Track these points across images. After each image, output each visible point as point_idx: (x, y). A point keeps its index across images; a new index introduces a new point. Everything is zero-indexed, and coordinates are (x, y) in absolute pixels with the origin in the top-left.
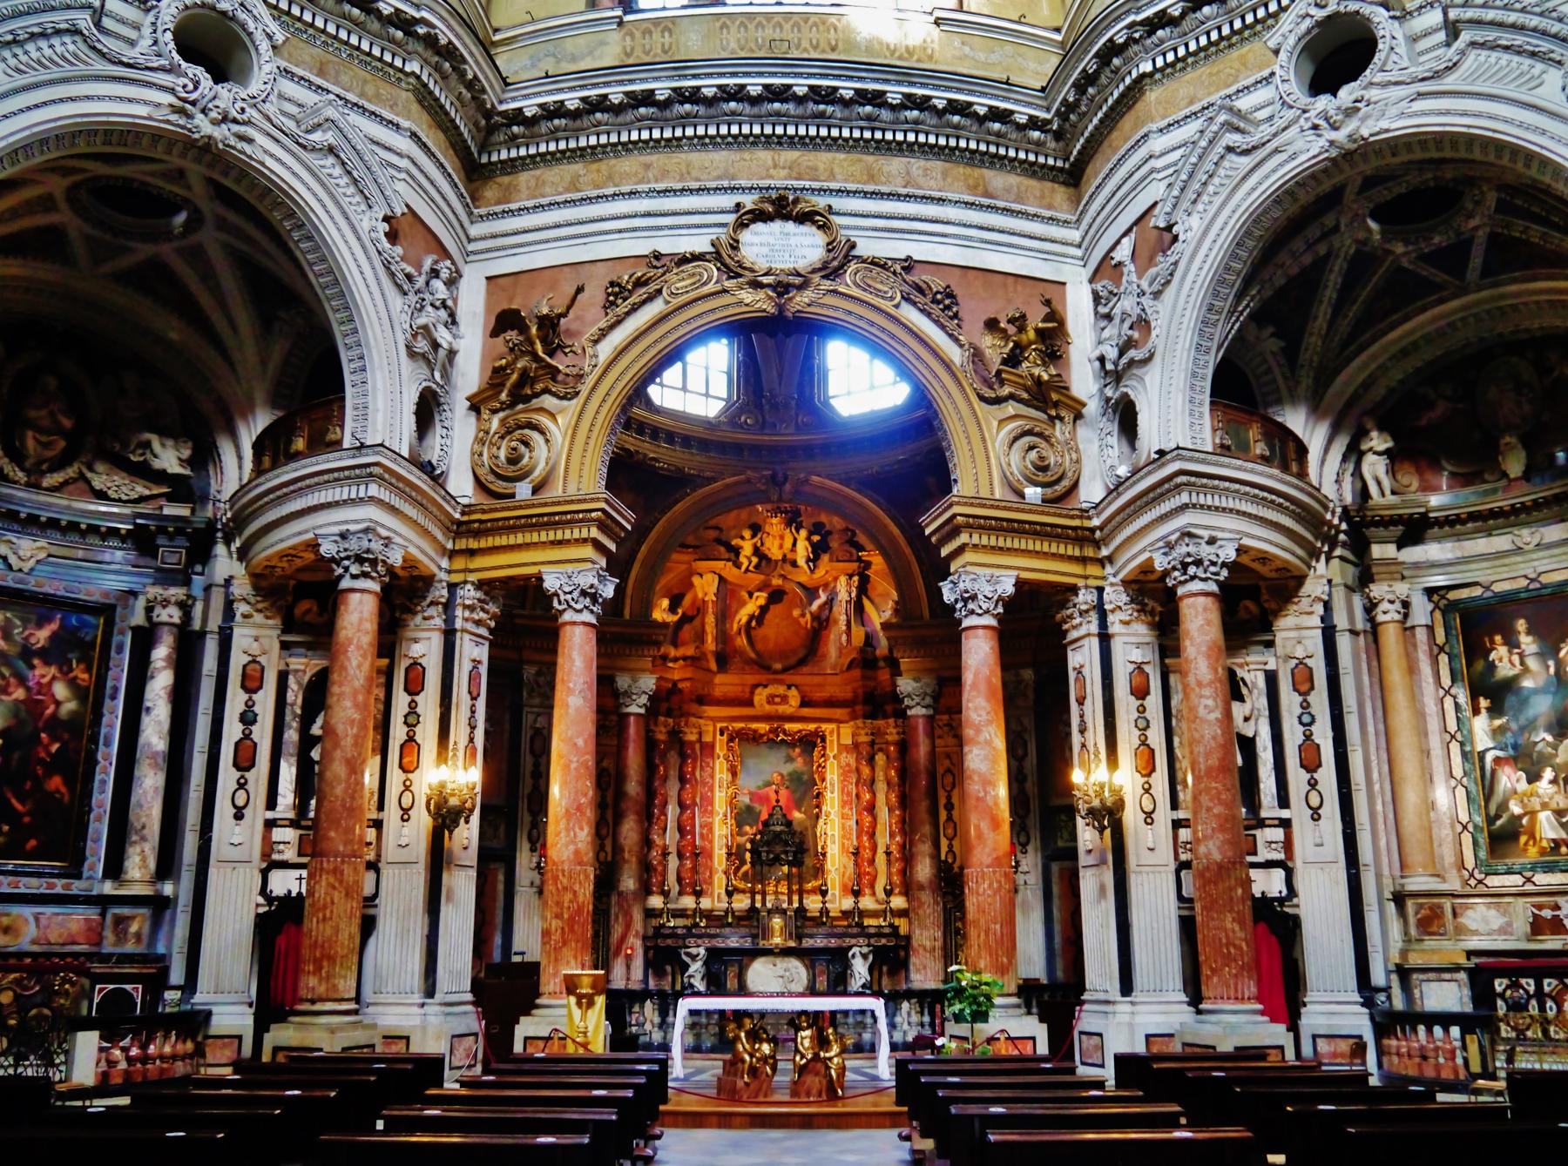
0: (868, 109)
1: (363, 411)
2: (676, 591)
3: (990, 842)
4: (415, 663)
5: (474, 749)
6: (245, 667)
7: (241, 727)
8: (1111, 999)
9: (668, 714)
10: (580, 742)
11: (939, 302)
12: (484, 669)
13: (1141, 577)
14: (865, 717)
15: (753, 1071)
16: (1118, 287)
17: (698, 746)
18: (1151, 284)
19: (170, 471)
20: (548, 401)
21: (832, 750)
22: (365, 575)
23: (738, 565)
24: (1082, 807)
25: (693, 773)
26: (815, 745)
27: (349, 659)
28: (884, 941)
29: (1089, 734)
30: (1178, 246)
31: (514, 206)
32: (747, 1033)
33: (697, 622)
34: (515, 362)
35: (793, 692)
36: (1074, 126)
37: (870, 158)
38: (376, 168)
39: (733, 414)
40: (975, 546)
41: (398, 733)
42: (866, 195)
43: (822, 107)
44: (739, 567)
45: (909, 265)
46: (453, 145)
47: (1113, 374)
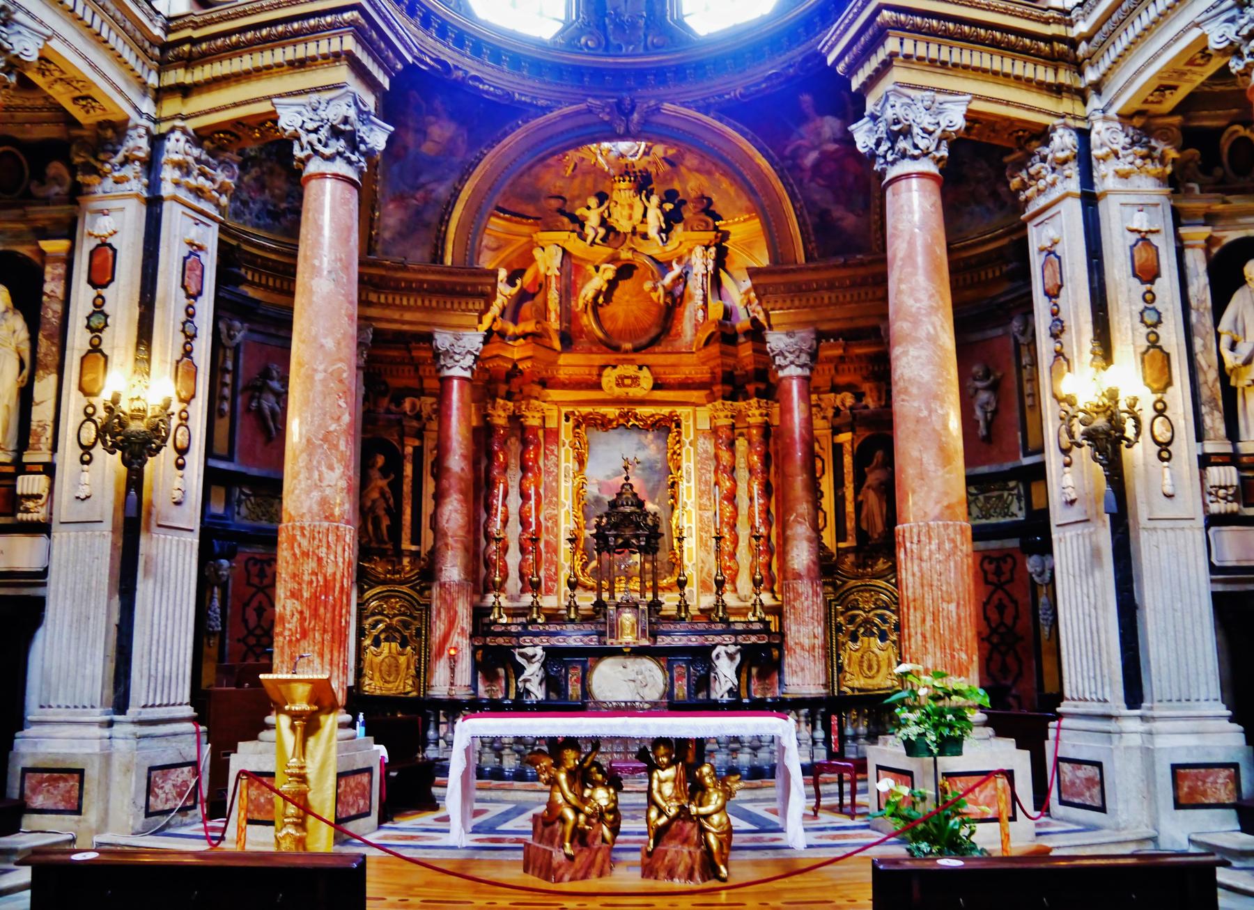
2: (516, 267)
3: (937, 483)
4: (104, 244)
8: (1114, 712)
9: (509, 396)
10: (329, 343)
12: (210, 260)
14: (725, 398)
15: (580, 837)
17: (541, 433)
21: (688, 434)
23: (583, 237)
25: (536, 460)
26: (669, 431)
28: (753, 639)
29: (1068, 338)
32: (571, 774)
33: (539, 299)
39: (570, 38)
40: (908, 57)
41: (78, 339)
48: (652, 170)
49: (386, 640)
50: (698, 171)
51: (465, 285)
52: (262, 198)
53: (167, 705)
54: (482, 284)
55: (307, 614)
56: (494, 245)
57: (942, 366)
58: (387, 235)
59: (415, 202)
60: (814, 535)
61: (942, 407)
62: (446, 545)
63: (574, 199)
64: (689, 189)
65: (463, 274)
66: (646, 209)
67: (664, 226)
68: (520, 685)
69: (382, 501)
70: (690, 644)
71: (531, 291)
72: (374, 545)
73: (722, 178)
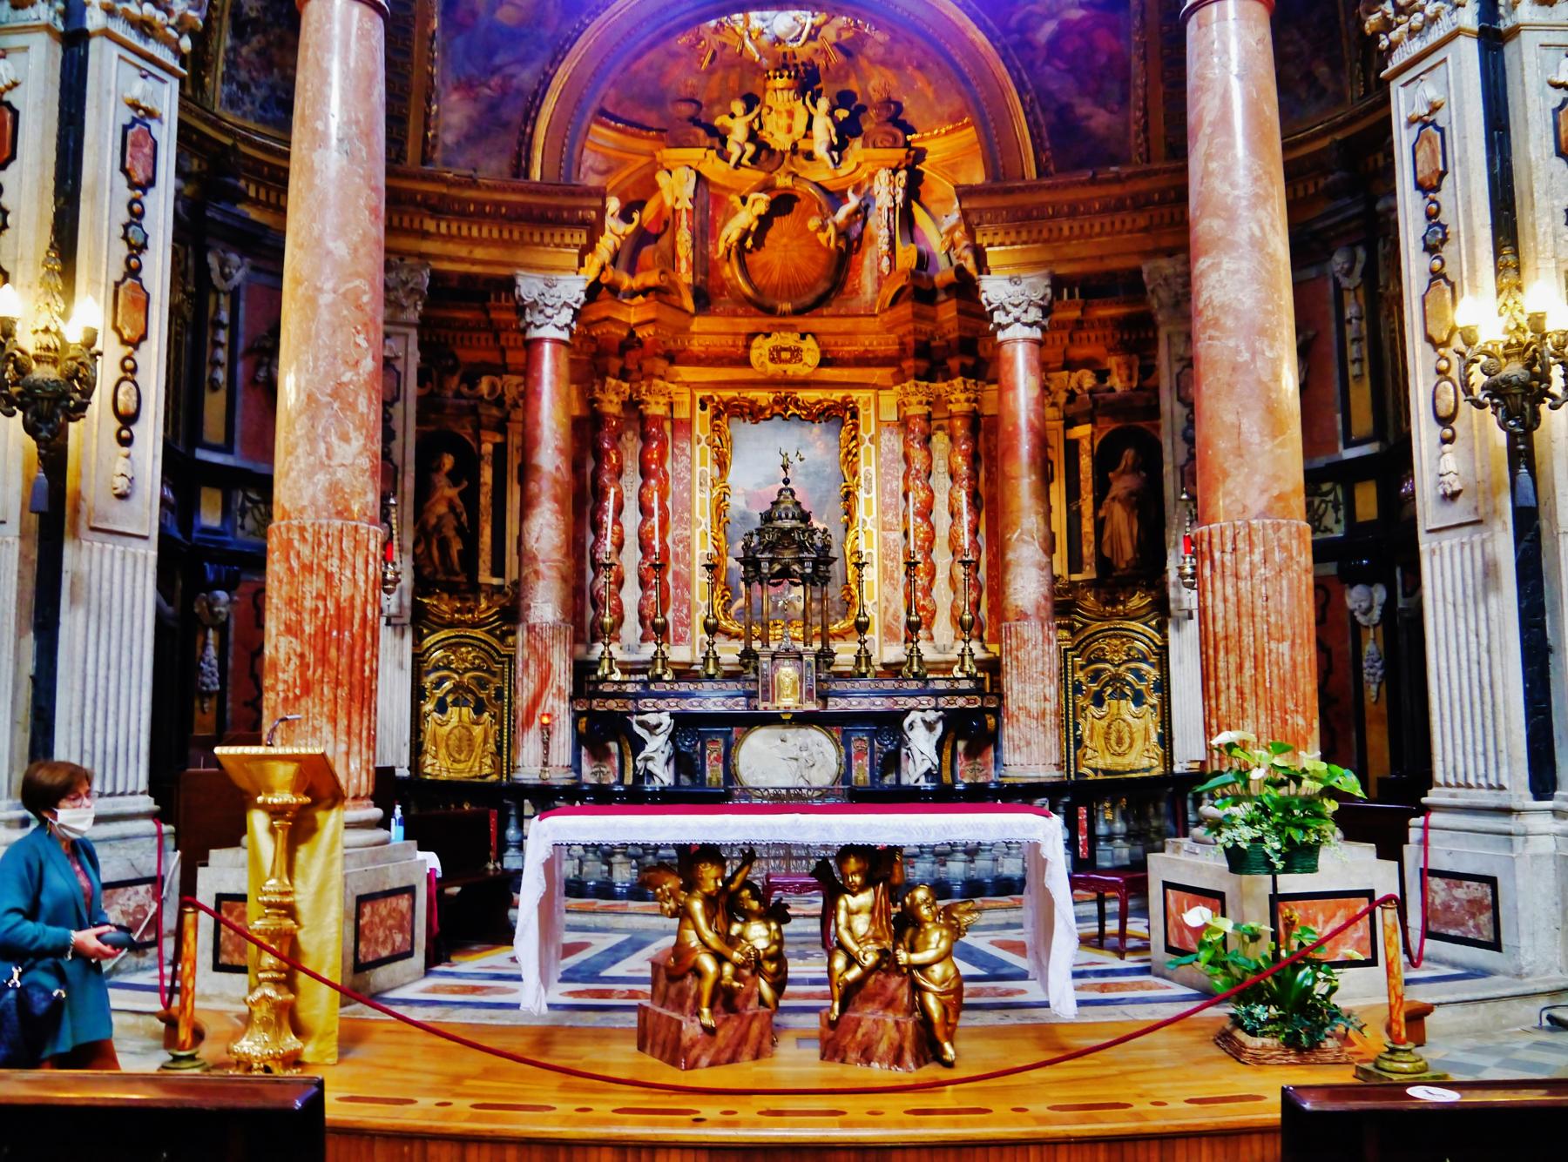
2: (632, 197)
8: (1515, 804)
9: (624, 375)
10: (340, 248)
14: (918, 377)
15: (725, 998)
17: (667, 426)
28: (961, 702)
32: (709, 900)
33: (664, 242)
35: (810, 342)
44: (727, 160)
48: (820, 62)
49: (455, 703)
50: (883, 63)
51: (559, 208)
52: (270, 81)
53: (110, 795)
54: (584, 208)
55: (310, 658)
56: (603, 167)
57: (1272, 285)
58: (449, 138)
59: (487, 91)
60: (1045, 559)
61: (1271, 347)
62: (536, 572)
63: (711, 103)
64: (870, 89)
65: (556, 194)
66: (811, 117)
67: (836, 141)
68: (640, 765)
69: (451, 517)
70: (873, 708)
71: (653, 230)
72: (441, 577)
73: (917, 74)
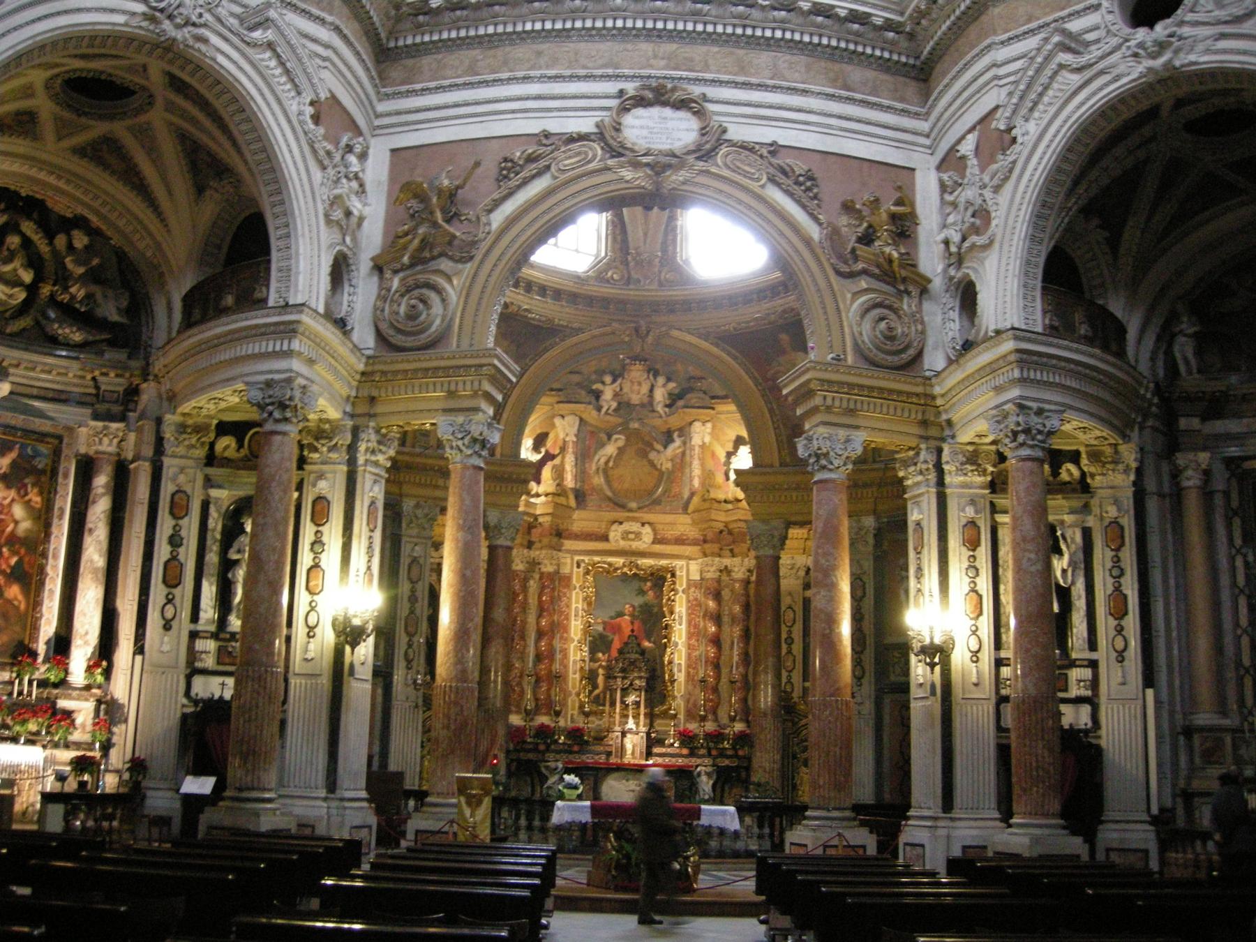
0: (741, 8)
1: (287, 273)
5: (371, 575)
6: (173, 495)
7: (169, 548)
11: (801, 184)
12: (380, 505)
13: (977, 440)
16: (963, 178)
18: (992, 179)
19: (110, 319)
20: (445, 264)
21: (681, 585)
22: (286, 420)
23: (599, 409)
24: (916, 646)
26: (664, 579)
27: (272, 494)
29: (925, 580)
30: (1017, 148)
31: (418, 86)
33: (557, 461)
34: (415, 228)
35: (647, 529)
36: (925, 30)
37: (741, 52)
38: (305, 60)
39: (600, 274)
41: (305, 559)
42: (736, 85)
43: (699, 6)
45: (775, 149)
46: (366, 33)
47: (958, 260)
